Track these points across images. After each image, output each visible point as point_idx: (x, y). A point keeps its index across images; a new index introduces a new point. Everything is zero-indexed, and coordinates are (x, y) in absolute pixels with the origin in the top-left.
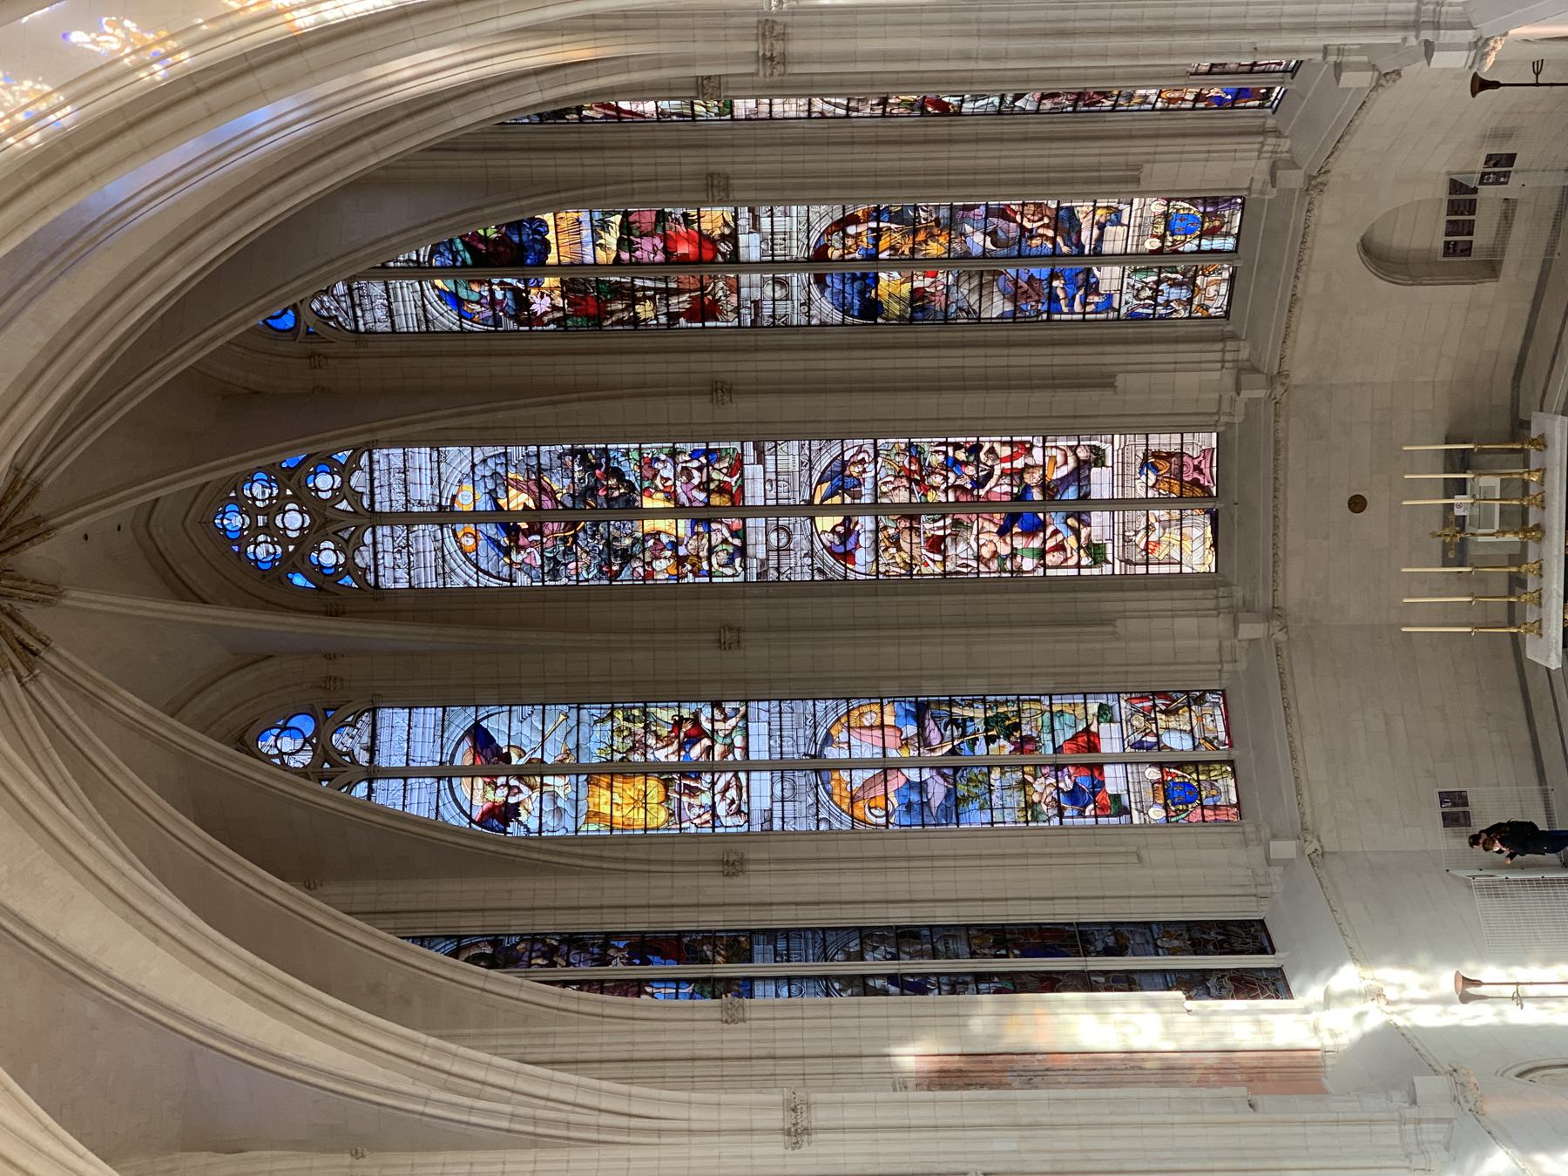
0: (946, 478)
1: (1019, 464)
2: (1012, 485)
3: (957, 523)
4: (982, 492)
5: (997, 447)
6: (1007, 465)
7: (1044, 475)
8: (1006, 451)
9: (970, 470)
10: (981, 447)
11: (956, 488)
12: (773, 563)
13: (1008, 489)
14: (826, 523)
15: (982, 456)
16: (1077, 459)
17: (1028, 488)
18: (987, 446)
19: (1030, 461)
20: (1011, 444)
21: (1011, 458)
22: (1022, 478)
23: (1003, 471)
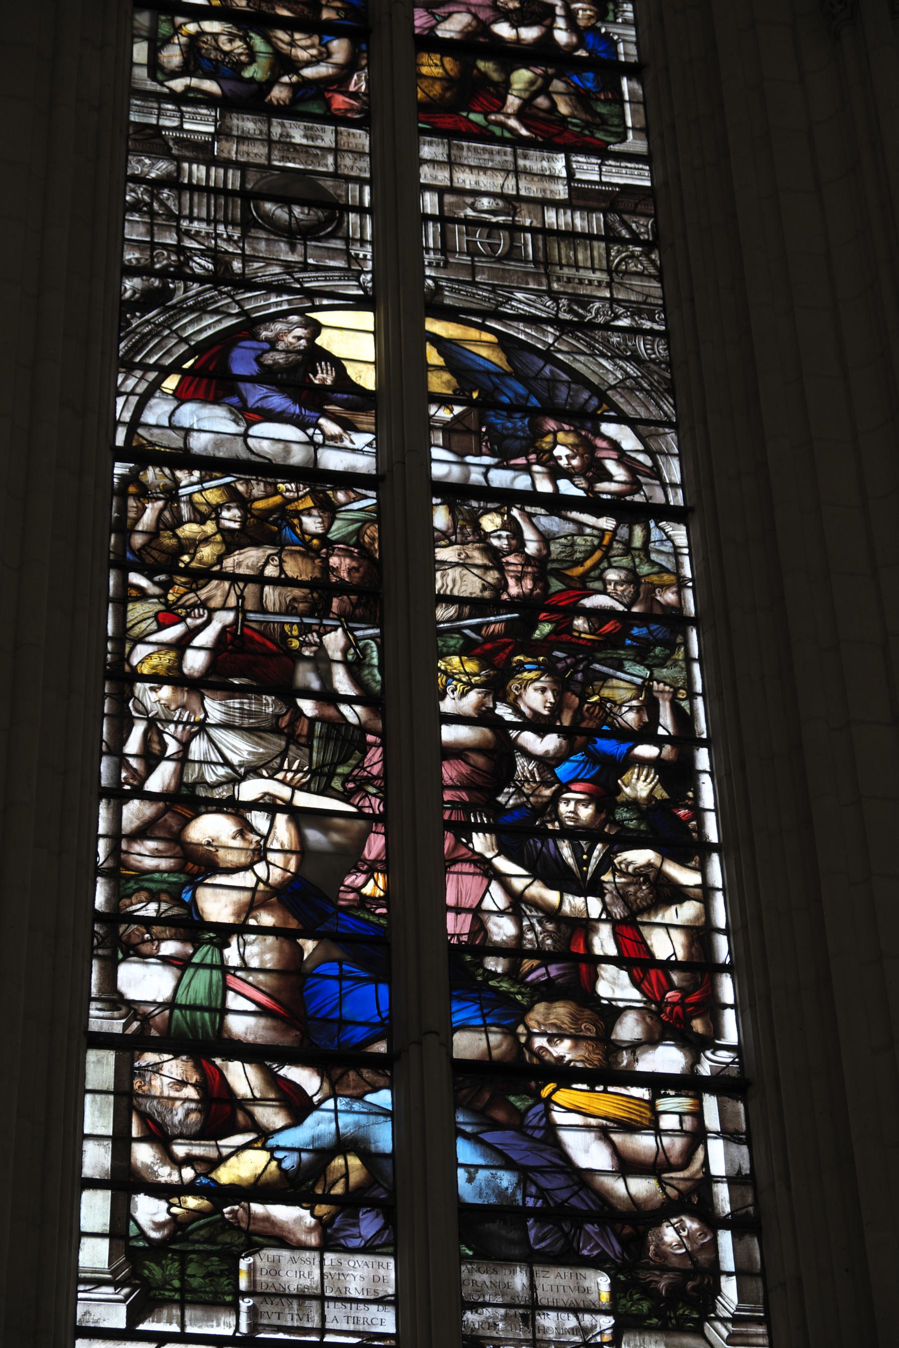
0: (539, 725)
1: (614, 985)
2: (513, 951)
3: (345, 741)
4: (480, 843)
5: (688, 911)
6: (604, 942)
7: (565, 1075)
8: (665, 945)
9: (576, 809)
10: (683, 862)
11: (500, 751)
12: (199, 172)
13: (503, 929)
14: (351, 339)
15: (641, 857)
16: (644, 1218)
17: (504, 1010)
18: (687, 877)
19: (629, 1029)
20: (700, 964)
21: (636, 960)
22: (548, 992)
23: (584, 926)
